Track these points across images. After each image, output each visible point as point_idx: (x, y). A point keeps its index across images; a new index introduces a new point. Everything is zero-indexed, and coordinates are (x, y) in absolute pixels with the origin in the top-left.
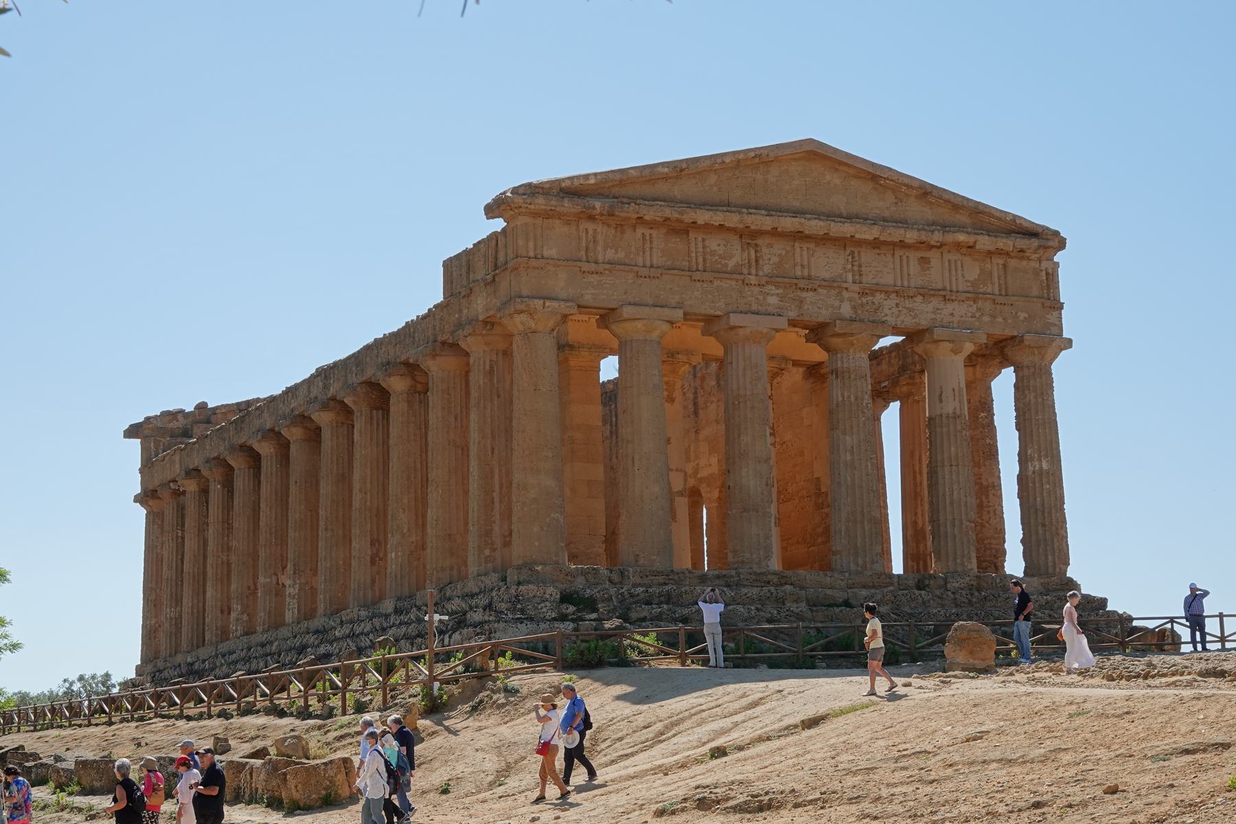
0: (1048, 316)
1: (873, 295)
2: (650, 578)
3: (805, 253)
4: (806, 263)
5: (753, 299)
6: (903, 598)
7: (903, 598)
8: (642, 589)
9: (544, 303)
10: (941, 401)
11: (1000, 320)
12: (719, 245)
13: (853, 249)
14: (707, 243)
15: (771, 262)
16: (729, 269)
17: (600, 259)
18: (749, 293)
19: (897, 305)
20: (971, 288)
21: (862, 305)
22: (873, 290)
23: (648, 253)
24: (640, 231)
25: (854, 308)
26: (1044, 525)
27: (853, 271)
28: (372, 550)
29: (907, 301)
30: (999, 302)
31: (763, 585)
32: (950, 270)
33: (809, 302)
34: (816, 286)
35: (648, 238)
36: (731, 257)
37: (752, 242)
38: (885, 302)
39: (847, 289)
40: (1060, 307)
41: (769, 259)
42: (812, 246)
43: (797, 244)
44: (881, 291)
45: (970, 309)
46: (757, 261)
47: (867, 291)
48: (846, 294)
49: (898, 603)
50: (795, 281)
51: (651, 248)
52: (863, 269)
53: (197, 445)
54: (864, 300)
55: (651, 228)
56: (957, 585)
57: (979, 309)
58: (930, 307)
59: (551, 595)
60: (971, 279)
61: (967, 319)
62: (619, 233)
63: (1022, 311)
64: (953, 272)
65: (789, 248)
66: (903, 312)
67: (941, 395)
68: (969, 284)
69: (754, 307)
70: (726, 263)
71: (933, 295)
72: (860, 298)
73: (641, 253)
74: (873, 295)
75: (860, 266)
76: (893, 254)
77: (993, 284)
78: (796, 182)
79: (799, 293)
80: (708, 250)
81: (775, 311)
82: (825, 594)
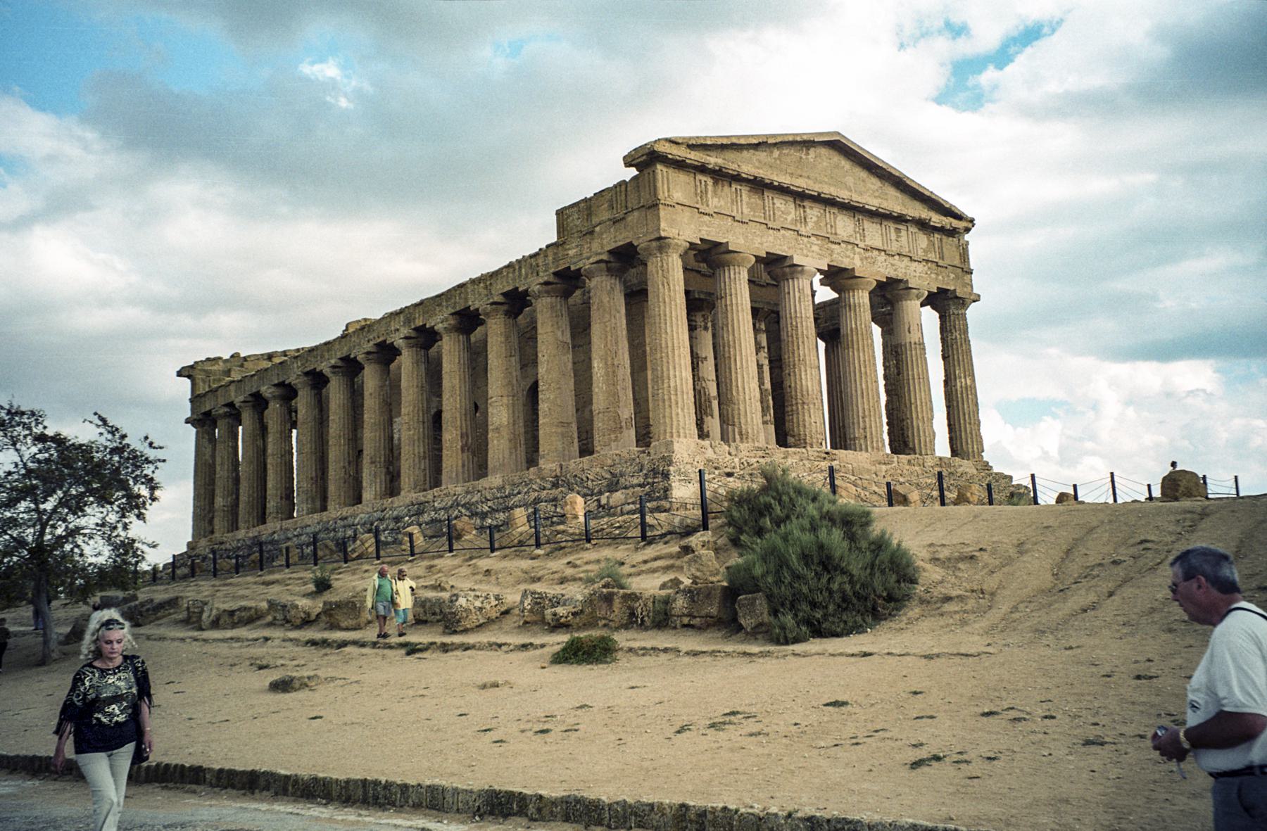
3: (832, 216)
10: (909, 332)
11: (940, 277)
14: (775, 201)
15: (813, 220)
19: (885, 260)
21: (866, 258)
25: (861, 259)
26: (970, 424)
28: (462, 441)
36: (789, 213)
38: (879, 258)
42: (836, 211)
46: (805, 218)
51: (741, 201)
53: (256, 377)
56: (929, 464)
57: (929, 268)
65: (822, 211)
67: (909, 329)
74: (872, 252)
75: (864, 230)
78: (825, 164)
79: (830, 245)
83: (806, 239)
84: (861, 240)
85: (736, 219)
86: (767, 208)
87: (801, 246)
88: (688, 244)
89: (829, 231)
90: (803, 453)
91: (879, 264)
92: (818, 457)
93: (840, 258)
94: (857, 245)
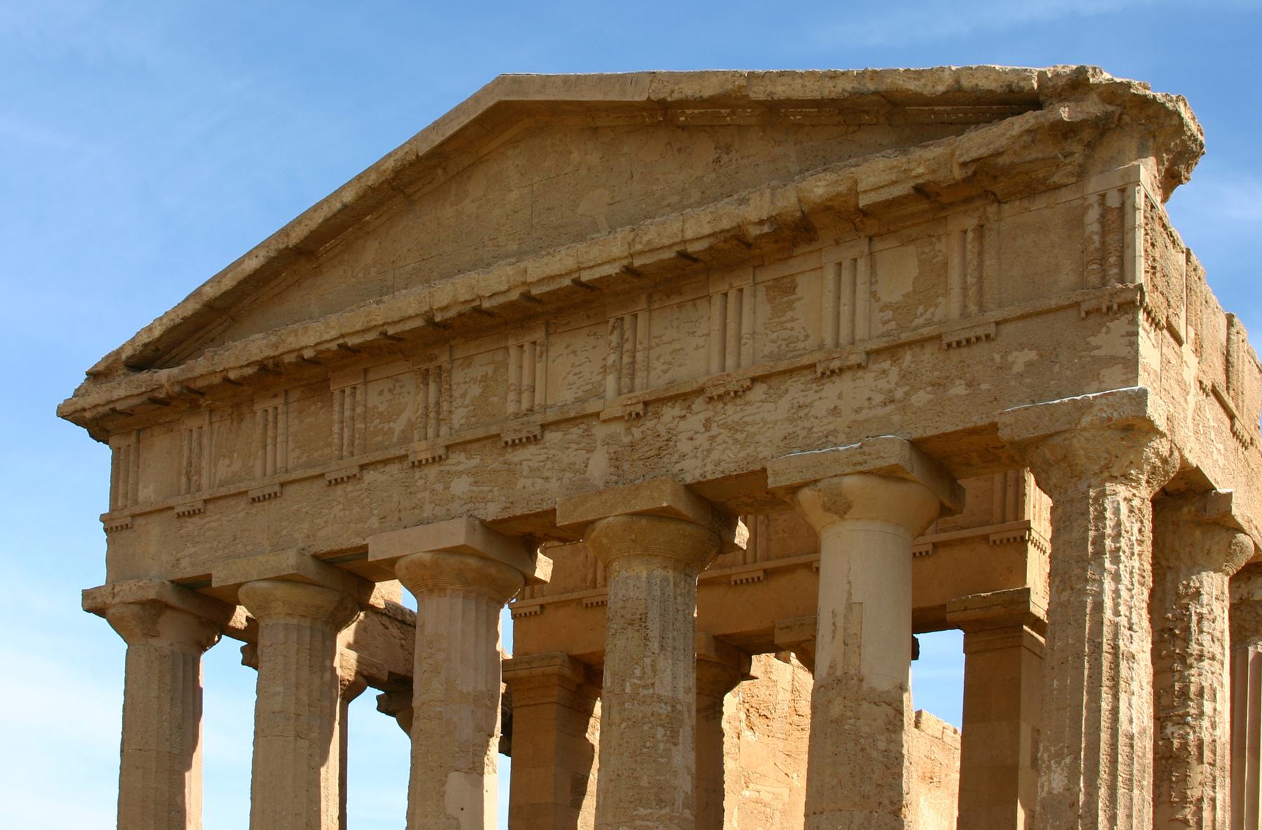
0: (1093, 341)
1: (657, 415)
3: (526, 356)
4: (526, 381)
5: (427, 494)
11: (959, 389)
13: (619, 314)
16: (395, 439)
18: (421, 482)
19: (707, 424)
21: (632, 446)
22: (652, 405)
25: (615, 460)
29: (730, 409)
30: (953, 339)
34: (537, 431)
35: (270, 418)
37: (431, 366)
38: (682, 425)
41: (463, 396)
42: (539, 335)
44: (673, 399)
45: (882, 384)
46: (438, 404)
47: (639, 408)
48: (600, 431)
50: (494, 430)
52: (640, 356)
54: (637, 433)
55: (275, 396)
58: (784, 406)
60: (896, 297)
62: (235, 423)
63: (1021, 347)
66: (719, 439)
69: (428, 512)
70: (390, 429)
73: (260, 453)
75: (634, 351)
76: (709, 298)
77: (946, 293)
80: (359, 410)
83: (433, 471)
84: (619, 393)
85: (253, 494)
88: (136, 608)
89: (511, 408)
91: (684, 446)
94: (597, 415)
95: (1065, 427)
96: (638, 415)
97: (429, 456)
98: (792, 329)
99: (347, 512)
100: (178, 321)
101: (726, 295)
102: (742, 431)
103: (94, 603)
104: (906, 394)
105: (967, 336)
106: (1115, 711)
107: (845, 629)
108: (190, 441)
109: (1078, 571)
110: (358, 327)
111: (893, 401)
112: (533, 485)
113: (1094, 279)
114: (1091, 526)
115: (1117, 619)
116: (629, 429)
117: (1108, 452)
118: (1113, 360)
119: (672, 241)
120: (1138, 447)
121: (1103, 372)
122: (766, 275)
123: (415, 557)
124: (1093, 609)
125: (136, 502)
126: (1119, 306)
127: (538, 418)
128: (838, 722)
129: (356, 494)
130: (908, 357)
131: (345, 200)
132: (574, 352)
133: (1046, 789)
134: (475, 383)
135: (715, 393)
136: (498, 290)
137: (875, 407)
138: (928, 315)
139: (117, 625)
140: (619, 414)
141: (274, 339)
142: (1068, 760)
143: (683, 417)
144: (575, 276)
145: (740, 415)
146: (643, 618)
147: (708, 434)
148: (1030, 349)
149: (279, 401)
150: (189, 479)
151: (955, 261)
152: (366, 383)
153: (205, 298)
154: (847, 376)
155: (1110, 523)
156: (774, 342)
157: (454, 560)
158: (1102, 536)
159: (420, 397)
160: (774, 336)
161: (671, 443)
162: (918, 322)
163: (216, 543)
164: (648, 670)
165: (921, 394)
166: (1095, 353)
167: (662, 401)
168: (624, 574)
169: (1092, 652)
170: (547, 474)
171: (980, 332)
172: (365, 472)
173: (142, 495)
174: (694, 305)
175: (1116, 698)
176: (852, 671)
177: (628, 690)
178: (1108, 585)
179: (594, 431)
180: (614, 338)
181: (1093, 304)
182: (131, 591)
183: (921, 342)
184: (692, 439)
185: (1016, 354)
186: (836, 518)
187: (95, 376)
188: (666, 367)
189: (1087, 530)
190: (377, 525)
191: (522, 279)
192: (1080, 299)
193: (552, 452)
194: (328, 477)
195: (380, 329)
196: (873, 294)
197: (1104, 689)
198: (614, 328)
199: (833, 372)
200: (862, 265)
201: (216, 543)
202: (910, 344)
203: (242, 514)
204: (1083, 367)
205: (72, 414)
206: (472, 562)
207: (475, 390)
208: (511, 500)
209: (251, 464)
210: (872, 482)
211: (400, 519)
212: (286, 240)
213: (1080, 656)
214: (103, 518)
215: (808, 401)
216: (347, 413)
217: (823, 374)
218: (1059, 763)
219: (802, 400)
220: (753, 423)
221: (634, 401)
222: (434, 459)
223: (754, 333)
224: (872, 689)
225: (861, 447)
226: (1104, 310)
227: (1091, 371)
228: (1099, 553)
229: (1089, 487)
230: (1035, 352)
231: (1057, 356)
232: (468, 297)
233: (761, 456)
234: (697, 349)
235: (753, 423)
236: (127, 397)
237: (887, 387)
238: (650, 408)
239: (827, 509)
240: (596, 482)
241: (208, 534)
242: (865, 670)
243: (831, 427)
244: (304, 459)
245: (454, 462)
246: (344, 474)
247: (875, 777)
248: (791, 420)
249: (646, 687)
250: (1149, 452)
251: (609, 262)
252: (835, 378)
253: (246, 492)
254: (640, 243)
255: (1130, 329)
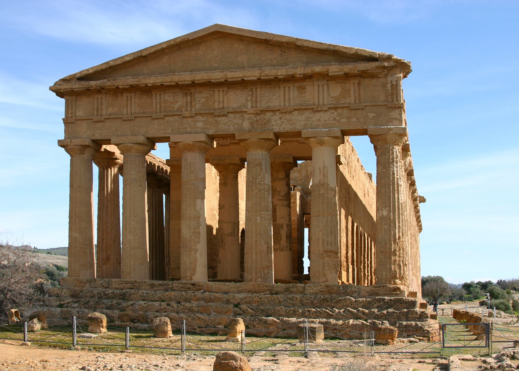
0: (390, 114)
1: (265, 114)
2: (123, 285)
3: (221, 94)
4: (221, 100)
5: (188, 125)
6: (266, 300)
7: (266, 300)
8: (111, 291)
9: (71, 140)
11: (354, 120)
12: (170, 96)
13: (251, 87)
14: (162, 96)
16: (175, 109)
17: (104, 113)
18: (185, 122)
19: (281, 118)
20: (334, 102)
21: (257, 121)
22: (264, 111)
23: (129, 107)
24: (125, 95)
25: (252, 124)
27: (252, 101)
29: (287, 115)
30: (353, 108)
31: (186, 290)
32: (319, 93)
33: (222, 123)
34: (226, 114)
35: (129, 98)
37: (188, 92)
38: (273, 118)
39: (246, 112)
40: (400, 107)
41: (199, 101)
43: (216, 90)
44: (270, 111)
45: (332, 115)
46: (191, 102)
47: (260, 112)
48: (246, 116)
49: (262, 302)
50: (212, 112)
51: (131, 104)
52: (258, 99)
54: (258, 118)
55: (131, 93)
56: (312, 291)
57: (339, 115)
58: (303, 117)
59: (65, 293)
60: (335, 95)
61: (330, 122)
62: (115, 98)
63: (371, 112)
64: (321, 93)
68: (333, 99)
69: (189, 130)
70: (174, 106)
71: (306, 109)
72: (256, 117)
73: (126, 107)
74: (265, 114)
75: (256, 97)
76: (280, 87)
77: (350, 96)
78: (216, 52)
79: (216, 118)
80: (163, 100)
81: (202, 130)
82: (215, 296)
83: (190, 120)
84: (252, 107)
85: (123, 119)
86: (154, 104)
87: (185, 125)
88: (79, 147)
89: (217, 106)
90: (169, 285)
91: (273, 123)
92: (182, 287)
93: (227, 127)
95: (386, 133)
96: (259, 113)
97: (189, 116)
98: (305, 98)
99: (159, 127)
100: (99, 69)
101: (284, 87)
102: (291, 121)
103: (61, 144)
104: (340, 119)
105: (357, 108)
106: (398, 198)
107: (323, 172)
108: (98, 101)
109: (388, 165)
110: (169, 81)
111: (336, 120)
112: (225, 127)
113: (390, 100)
114: (391, 155)
115: (398, 177)
116: (256, 116)
117: (395, 139)
118: (396, 119)
119: (273, 75)
120: (402, 139)
121: (393, 121)
122: (297, 84)
123: (187, 142)
124: (392, 174)
125: (76, 116)
126: (397, 107)
127: (227, 111)
128: (323, 194)
129: (162, 122)
130: (340, 110)
131: (163, 47)
132: (236, 95)
133: (381, 214)
134: (203, 98)
135: (283, 111)
136: (218, 78)
137: (331, 121)
138: (344, 101)
139: (67, 151)
140: (253, 112)
141: (137, 79)
142: (388, 208)
143: (273, 116)
144: (243, 78)
145: (291, 117)
146: (261, 164)
147: (280, 121)
148: (374, 113)
149: (133, 95)
150: (97, 112)
151: (352, 90)
152: (165, 93)
153: (110, 65)
154: (322, 113)
155: (395, 155)
156: (300, 101)
157: (199, 144)
158: (394, 158)
159: (185, 99)
160: (300, 99)
161: (269, 122)
162: (341, 102)
163: (109, 131)
164: (262, 177)
165: (344, 119)
166: (391, 116)
167: (266, 111)
168: (254, 152)
169: (392, 184)
170: (229, 124)
171: (360, 108)
172: (166, 117)
173: (78, 114)
174: (275, 88)
175: (398, 195)
176: (326, 183)
177: (257, 182)
178: (395, 169)
179: (244, 116)
180: (250, 93)
181: (391, 106)
182: (77, 142)
183: (344, 108)
184: (276, 121)
185: (369, 114)
186: (320, 145)
187: (64, 80)
188: (266, 102)
189: (390, 156)
190: (170, 132)
191: (226, 77)
192: (387, 104)
193: (230, 119)
194: (153, 117)
195: (176, 82)
196: (329, 94)
197: (396, 193)
198: (250, 91)
199: (318, 111)
200: (325, 87)
201: (109, 131)
202: (340, 107)
203: (119, 124)
204: (388, 119)
205: (51, 89)
206: (203, 144)
207: (203, 100)
208: (217, 130)
209: (121, 110)
210: (331, 139)
211: (179, 131)
212: (141, 54)
213: (389, 185)
214: (63, 119)
215: (311, 116)
216: (158, 101)
217: (315, 111)
218: (385, 209)
219: (309, 116)
220: (295, 120)
221: (258, 110)
222: (191, 116)
223: (294, 98)
224: (331, 187)
225: (329, 130)
226: (393, 107)
227: (390, 121)
228: (393, 161)
229: (390, 146)
230: (375, 114)
231: (381, 116)
232: (208, 79)
233: (297, 128)
234: (276, 99)
235: (295, 120)
236: (78, 88)
237: (334, 116)
238: (263, 112)
239: (318, 143)
240: (246, 129)
241: (105, 128)
242: (329, 183)
243: (318, 124)
244: (142, 111)
245: (197, 118)
246: (157, 117)
247: (333, 208)
248: (306, 121)
249: (262, 181)
250: (404, 140)
251: (253, 76)
252: (319, 112)
253: (122, 118)
254: (264, 73)
255: (400, 112)
